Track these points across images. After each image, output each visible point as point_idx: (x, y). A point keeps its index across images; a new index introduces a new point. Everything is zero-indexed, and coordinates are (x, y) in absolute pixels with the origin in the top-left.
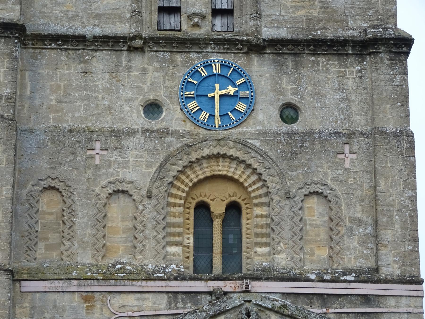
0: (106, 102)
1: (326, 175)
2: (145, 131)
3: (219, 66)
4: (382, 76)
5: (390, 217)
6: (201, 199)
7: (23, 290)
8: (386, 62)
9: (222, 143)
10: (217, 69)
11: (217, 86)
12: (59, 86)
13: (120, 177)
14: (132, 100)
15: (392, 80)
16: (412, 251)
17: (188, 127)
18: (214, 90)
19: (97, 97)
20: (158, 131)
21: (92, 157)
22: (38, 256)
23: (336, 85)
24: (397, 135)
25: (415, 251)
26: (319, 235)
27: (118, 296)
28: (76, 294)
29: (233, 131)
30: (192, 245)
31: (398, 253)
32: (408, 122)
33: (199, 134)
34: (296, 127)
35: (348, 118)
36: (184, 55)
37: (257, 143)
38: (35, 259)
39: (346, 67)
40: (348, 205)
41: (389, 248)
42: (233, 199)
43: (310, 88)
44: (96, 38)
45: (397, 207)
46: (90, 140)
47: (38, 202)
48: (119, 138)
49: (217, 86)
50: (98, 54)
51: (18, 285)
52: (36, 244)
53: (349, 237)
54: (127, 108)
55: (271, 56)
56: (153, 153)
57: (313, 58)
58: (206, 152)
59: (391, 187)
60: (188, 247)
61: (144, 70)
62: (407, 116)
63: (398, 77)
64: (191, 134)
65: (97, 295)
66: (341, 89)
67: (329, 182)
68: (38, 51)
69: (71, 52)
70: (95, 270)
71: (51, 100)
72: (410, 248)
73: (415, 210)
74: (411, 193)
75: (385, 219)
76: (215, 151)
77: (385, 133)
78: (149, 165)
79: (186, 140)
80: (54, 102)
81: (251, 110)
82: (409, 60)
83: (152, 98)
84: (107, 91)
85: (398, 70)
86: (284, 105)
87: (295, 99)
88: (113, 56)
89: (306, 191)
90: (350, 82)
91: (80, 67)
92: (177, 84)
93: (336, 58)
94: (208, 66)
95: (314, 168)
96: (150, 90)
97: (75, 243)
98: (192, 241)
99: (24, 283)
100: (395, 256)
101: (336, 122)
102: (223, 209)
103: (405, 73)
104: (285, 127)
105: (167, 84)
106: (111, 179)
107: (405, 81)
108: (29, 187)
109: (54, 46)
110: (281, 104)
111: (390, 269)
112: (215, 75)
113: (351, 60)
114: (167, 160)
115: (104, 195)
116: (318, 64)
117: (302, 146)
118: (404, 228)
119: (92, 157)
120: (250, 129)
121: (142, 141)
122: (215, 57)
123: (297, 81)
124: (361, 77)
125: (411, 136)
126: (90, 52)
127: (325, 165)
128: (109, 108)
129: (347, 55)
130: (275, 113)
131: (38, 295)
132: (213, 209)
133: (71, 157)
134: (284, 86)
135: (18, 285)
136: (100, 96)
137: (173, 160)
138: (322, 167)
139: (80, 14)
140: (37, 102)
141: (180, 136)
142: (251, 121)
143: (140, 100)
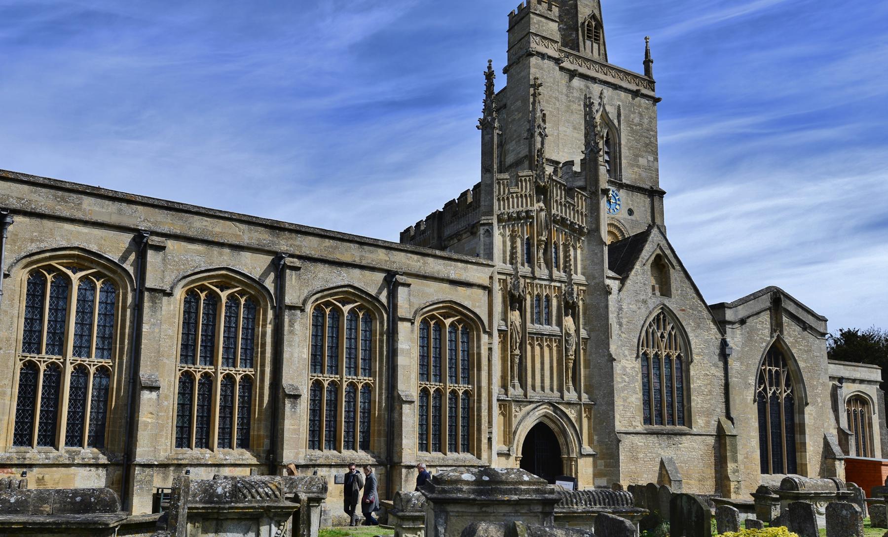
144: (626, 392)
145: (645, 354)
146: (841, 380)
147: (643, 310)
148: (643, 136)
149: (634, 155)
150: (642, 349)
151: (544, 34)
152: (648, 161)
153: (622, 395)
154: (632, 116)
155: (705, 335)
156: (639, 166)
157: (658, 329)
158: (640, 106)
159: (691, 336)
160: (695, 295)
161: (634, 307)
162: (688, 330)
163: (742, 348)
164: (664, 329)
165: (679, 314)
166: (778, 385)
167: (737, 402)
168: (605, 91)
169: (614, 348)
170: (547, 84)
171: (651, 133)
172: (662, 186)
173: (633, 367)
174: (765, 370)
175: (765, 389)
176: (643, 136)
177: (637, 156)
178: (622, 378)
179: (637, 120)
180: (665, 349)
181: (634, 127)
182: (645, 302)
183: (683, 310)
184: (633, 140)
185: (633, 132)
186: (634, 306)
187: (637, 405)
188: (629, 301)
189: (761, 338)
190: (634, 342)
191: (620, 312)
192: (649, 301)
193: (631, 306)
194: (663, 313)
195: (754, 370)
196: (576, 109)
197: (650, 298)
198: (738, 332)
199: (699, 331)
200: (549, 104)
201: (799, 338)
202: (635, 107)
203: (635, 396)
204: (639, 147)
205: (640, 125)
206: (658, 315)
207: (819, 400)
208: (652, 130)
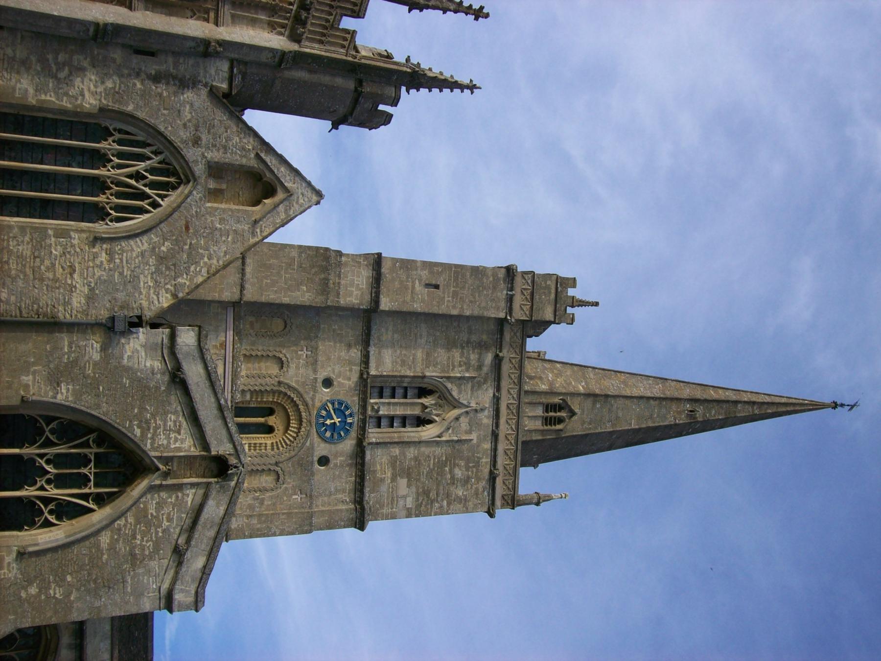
1: (289, 483)
2: (316, 379)
3: (351, 421)
4: (343, 514)
5: (265, 522)
6: (277, 411)
7: (229, 308)
8: (351, 516)
9: (308, 424)
10: (349, 420)
11: (339, 420)
12: (342, 330)
13: (291, 365)
14: (334, 372)
15: (342, 520)
16: (245, 535)
17: (318, 404)
18: (338, 418)
19: (336, 352)
20: (316, 387)
22: (247, 317)
23: (339, 488)
24: (311, 524)
25: (245, 537)
27: (223, 363)
28: (224, 339)
29: (315, 430)
30: (250, 406)
31: (243, 527)
32: (318, 530)
33: (313, 410)
34: (316, 466)
36: (357, 401)
37: (308, 444)
38: (246, 315)
39: (349, 494)
40: (271, 497)
42: (276, 430)
44: (368, 352)
45: (270, 526)
46: (312, 347)
47: (278, 317)
48: (312, 364)
49: (339, 420)
50: (360, 353)
51: (231, 305)
52: (254, 316)
53: (253, 498)
54: (329, 369)
55: (356, 451)
56: (304, 384)
57: (354, 474)
58: (303, 414)
59: (282, 522)
60: (249, 404)
61: (349, 379)
62: (321, 529)
63: (343, 523)
64: (313, 405)
65: (223, 351)
67: (285, 486)
68: (362, 319)
69: (361, 337)
70: (238, 350)
71: (335, 326)
72: (247, 534)
73: (268, 536)
74: (277, 533)
75: (263, 519)
77: (312, 517)
78: (297, 382)
80: (333, 327)
81: (325, 440)
82: (353, 529)
83: (335, 383)
84: (339, 357)
85: (346, 523)
86: (328, 458)
87: (331, 465)
88: (358, 361)
89: (280, 472)
90: (340, 496)
92: (341, 397)
93: (354, 487)
94: (351, 415)
96: (339, 382)
97: (254, 339)
98: (253, 406)
99: (232, 308)
100: (242, 525)
101: (318, 489)
102: (270, 423)
103: (345, 527)
104: (316, 459)
105: (342, 392)
106: (289, 360)
107: (340, 527)
108: (287, 312)
109: (364, 328)
110: (329, 456)
111: (234, 523)
112: (346, 419)
113: (352, 496)
114: (299, 392)
116: (351, 477)
117: (305, 469)
118: (258, 529)
120: (315, 439)
121: (312, 378)
122: (356, 419)
123: (342, 466)
124: (343, 502)
125: (310, 532)
126: (360, 348)
127: (294, 483)
129: (355, 493)
130: (324, 453)
131: (225, 317)
132: (270, 417)
133: (303, 337)
134: (339, 458)
135: (231, 305)
136: (336, 354)
137: (299, 396)
138: (293, 481)
139: (381, 343)
140: (334, 318)
141: (313, 399)
143: (333, 376)
144: (39, 69)
145: (106, 134)
147: (184, 134)
148: (438, 485)
149: (409, 468)
150: (115, 130)
151: (536, 297)
152: (405, 497)
153: (33, 59)
154: (462, 463)
155: (146, 281)
156: (394, 479)
157: (152, 171)
158: (478, 479)
159: (141, 245)
160: (221, 263)
161: (187, 114)
162: (154, 237)
163: (128, 369)
164: (153, 185)
165: (178, 221)
166: (60, 481)
167: (23, 347)
168: (486, 413)
169: (116, 56)
170: (477, 295)
171: (445, 503)
172: (371, 525)
173: (83, 95)
174: (86, 445)
175: (48, 443)
176: (438, 485)
177: (407, 473)
178: (64, 64)
179: (459, 473)
180: (119, 184)
181: (447, 469)
182: (196, 142)
183: (187, 228)
184: (429, 466)
185: (441, 465)
186: (189, 116)
187: (14, 89)
188: (197, 105)
189: (148, 422)
190: (127, 105)
191: (177, 82)
192: (200, 150)
193: (188, 107)
194: (179, 184)
195: (87, 404)
196: (453, 356)
197: (203, 154)
198: (157, 365)
199: (152, 261)
200: (453, 298)
201: (157, 533)
202: (475, 470)
203: (31, 91)
204: (423, 479)
205: (453, 481)
206: (174, 173)
207: (33, 590)
208: (449, 504)
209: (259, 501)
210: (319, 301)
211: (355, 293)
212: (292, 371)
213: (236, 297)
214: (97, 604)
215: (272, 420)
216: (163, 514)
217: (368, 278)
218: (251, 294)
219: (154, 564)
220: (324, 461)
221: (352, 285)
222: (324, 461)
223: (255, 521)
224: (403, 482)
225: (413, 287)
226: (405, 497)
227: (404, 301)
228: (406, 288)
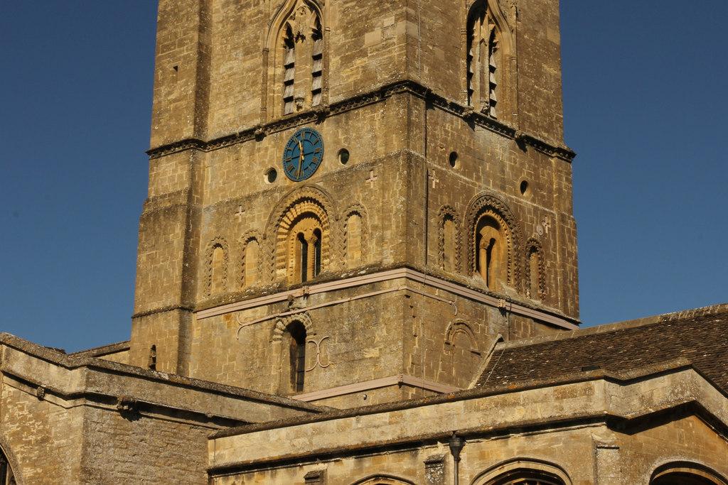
0: (247, 177)
8: (395, 102)
21: (237, 218)
26: (356, 243)
35: (374, 151)
41: (389, 244)
43: (354, 135)
46: (236, 206)
58: (295, 198)
64: (288, 187)
66: (372, 130)
67: (361, 202)
76: (299, 196)
79: (285, 193)
87: (345, 145)
89: (348, 213)
90: (377, 123)
91: (234, 156)
95: (352, 193)
115: (243, 242)
119: (237, 218)
128: (248, 181)
142: (320, 168)
146: (457, 440)
184: (353, 7)
196: (250, 17)
209: (374, 232)
210: (181, 215)
211: (179, 172)
212: (255, 225)
213: (176, 313)
214: (70, 473)
215: (308, 235)
216: (19, 416)
217: (168, 161)
218: (174, 299)
219: (51, 417)
220: (344, 155)
221: (172, 179)
222: (344, 155)
223: (388, 234)
224: (370, 38)
225: (175, 101)
226: (384, 29)
227: (187, 108)
228: (176, 108)
